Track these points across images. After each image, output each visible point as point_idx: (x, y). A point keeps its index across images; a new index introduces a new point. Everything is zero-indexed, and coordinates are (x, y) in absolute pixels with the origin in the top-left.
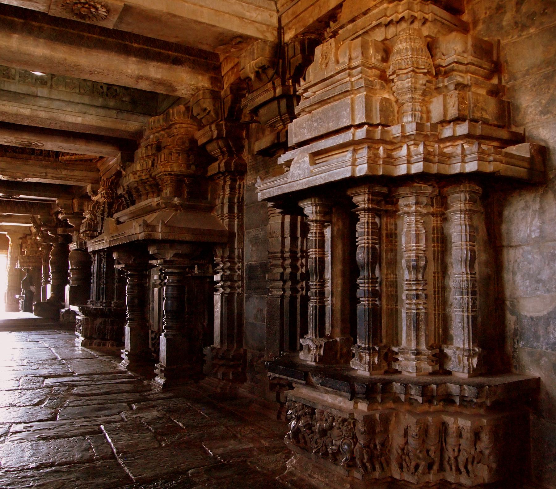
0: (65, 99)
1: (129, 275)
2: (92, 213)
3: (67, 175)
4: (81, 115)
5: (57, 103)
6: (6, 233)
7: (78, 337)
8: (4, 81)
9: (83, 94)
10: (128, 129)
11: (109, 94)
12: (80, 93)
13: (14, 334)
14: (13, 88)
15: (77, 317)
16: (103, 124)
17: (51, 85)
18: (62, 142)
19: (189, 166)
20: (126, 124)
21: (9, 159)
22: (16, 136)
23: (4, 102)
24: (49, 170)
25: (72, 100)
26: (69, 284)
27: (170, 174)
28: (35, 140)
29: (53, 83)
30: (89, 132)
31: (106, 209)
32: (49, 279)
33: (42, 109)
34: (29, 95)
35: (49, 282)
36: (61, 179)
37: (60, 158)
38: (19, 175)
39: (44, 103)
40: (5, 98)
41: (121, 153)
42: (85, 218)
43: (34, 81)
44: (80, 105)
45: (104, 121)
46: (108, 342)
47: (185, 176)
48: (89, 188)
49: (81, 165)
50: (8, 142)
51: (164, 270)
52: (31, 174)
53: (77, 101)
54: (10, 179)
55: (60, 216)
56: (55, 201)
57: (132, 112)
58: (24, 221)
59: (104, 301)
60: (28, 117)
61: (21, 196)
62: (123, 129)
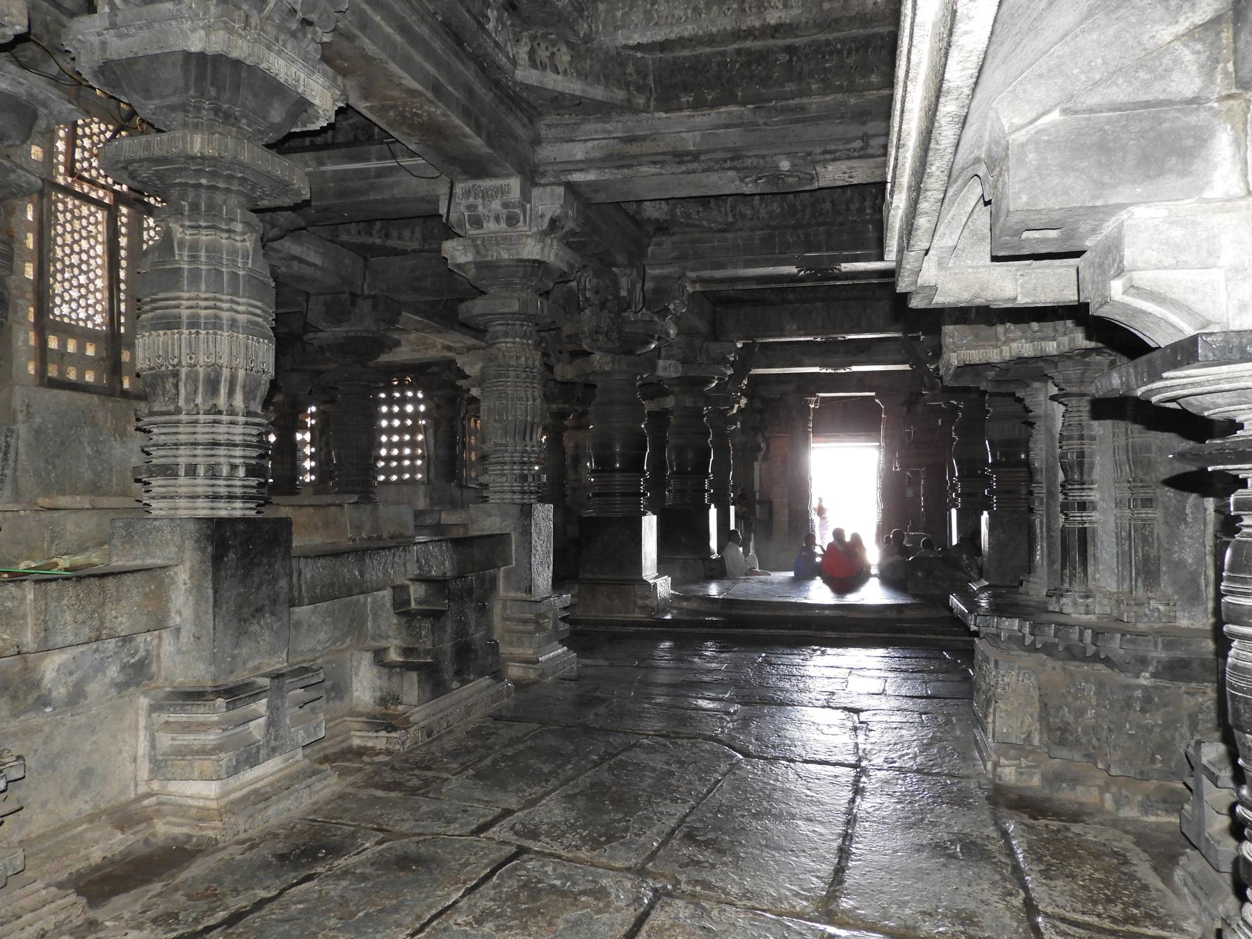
52: (818, 150)
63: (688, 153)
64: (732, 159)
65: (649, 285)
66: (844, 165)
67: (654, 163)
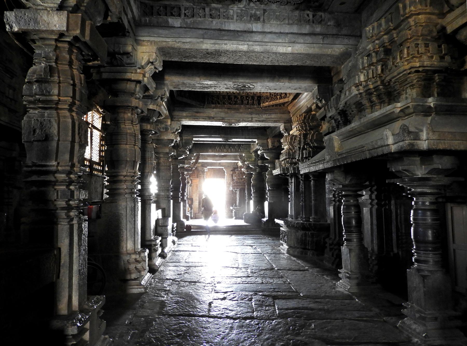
0: (277, 31)
1: (345, 196)
2: (291, 144)
3: (267, 118)
4: (291, 45)
5: (269, 36)
6: (223, 168)
7: (282, 245)
8: (225, 22)
9: (292, 24)
10: (334, 53)
11: (315, 22)
12: (288, 24)
13: (234, 237)
14: (232, 27)
15: (281, 228)
16: (311, 51)
17: (264, 20)
18: (269, 82)
19: (442, 58)
20: (332, 48)
21: (226, 110)
22: (234, 81)
23: (226, 42)
24: (253, 116)
25: (282, 31)
26: (267, 200)
27: (417, 72)
28: (248, 83)
29: (265, 18)
30: (296, 64)
31: (302, 140)
32: (252, 197)
33: (257, 43)
34: (245, 32)
35: (251, 199)
36: (262, 121)
37: (261, 105)
38: (233, 121)
39: (258, 37)
40: (226, 38)
41: (318, 86)
42: (284, 149)
43: (249, 18)
44: (289, 35)
45: (311, 47)
46: (309, 251)
47: (435, 72)
48: (282, 127)
49: (276, 109)
50: (228, 88)
51: (410, 190)
52: (242, 119)
53: (287, 31)
54: (228, 125)
55: (259, 152)
56: (255, 142)
57: (336, 36)
58: (234, 159)
59: (304, 216)
60: (246, 53)
61: (234, 140)
62: (329, 53)
63: (211, 117)
64: (222, 119)
65: (183, 141)
66: (246, 123)
67: (203, 118)
